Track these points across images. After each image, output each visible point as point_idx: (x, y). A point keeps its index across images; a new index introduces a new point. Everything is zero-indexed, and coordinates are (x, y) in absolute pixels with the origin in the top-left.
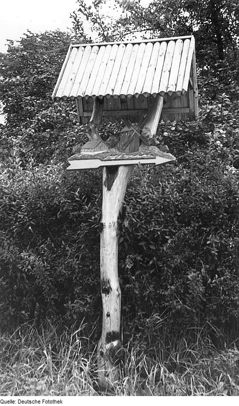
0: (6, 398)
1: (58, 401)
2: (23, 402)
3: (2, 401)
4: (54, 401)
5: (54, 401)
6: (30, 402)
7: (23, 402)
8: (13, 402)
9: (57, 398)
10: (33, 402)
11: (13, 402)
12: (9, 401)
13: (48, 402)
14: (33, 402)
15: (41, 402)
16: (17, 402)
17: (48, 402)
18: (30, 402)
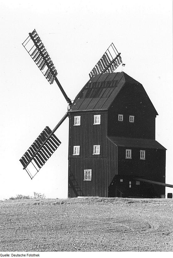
0: (4, 253)
1: (37, 255)
2: (14, 255)
3: (1, 255)
4: (34, 255)
5: (34, 255)
6: (19, 256)
7: (14, 255)
8: (8, 255)
9: (36, 253)
10: (21, 256)
11: (8, 255)
12: (5, 255)
13: (31, 255)
14: (21, 256)
15: (26, 255)
16: (11, 255)
17: (31, 255)
18: (19, 256)
